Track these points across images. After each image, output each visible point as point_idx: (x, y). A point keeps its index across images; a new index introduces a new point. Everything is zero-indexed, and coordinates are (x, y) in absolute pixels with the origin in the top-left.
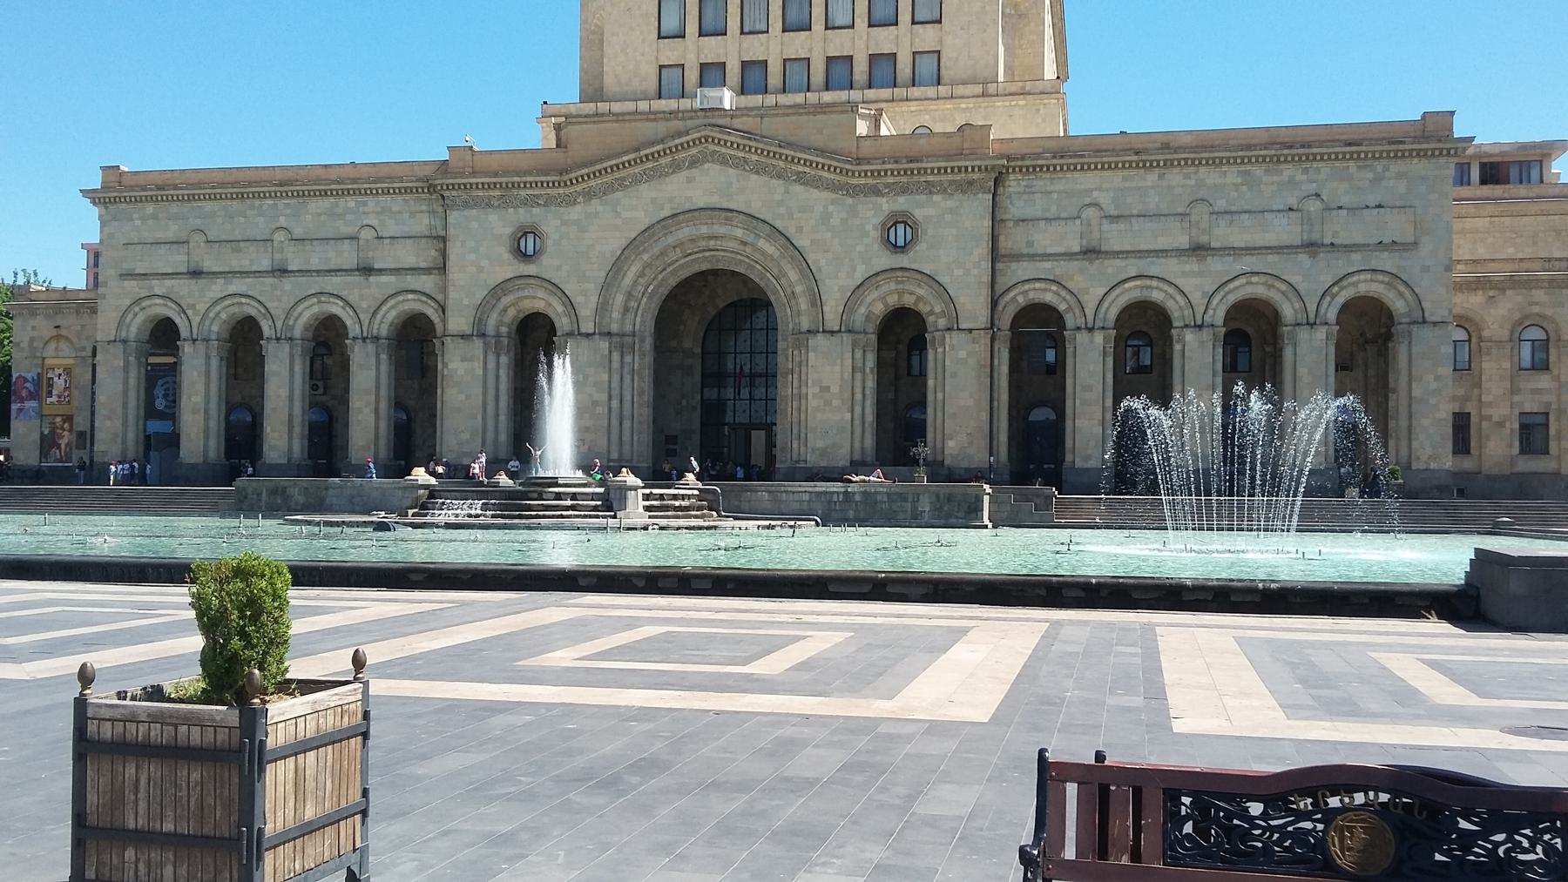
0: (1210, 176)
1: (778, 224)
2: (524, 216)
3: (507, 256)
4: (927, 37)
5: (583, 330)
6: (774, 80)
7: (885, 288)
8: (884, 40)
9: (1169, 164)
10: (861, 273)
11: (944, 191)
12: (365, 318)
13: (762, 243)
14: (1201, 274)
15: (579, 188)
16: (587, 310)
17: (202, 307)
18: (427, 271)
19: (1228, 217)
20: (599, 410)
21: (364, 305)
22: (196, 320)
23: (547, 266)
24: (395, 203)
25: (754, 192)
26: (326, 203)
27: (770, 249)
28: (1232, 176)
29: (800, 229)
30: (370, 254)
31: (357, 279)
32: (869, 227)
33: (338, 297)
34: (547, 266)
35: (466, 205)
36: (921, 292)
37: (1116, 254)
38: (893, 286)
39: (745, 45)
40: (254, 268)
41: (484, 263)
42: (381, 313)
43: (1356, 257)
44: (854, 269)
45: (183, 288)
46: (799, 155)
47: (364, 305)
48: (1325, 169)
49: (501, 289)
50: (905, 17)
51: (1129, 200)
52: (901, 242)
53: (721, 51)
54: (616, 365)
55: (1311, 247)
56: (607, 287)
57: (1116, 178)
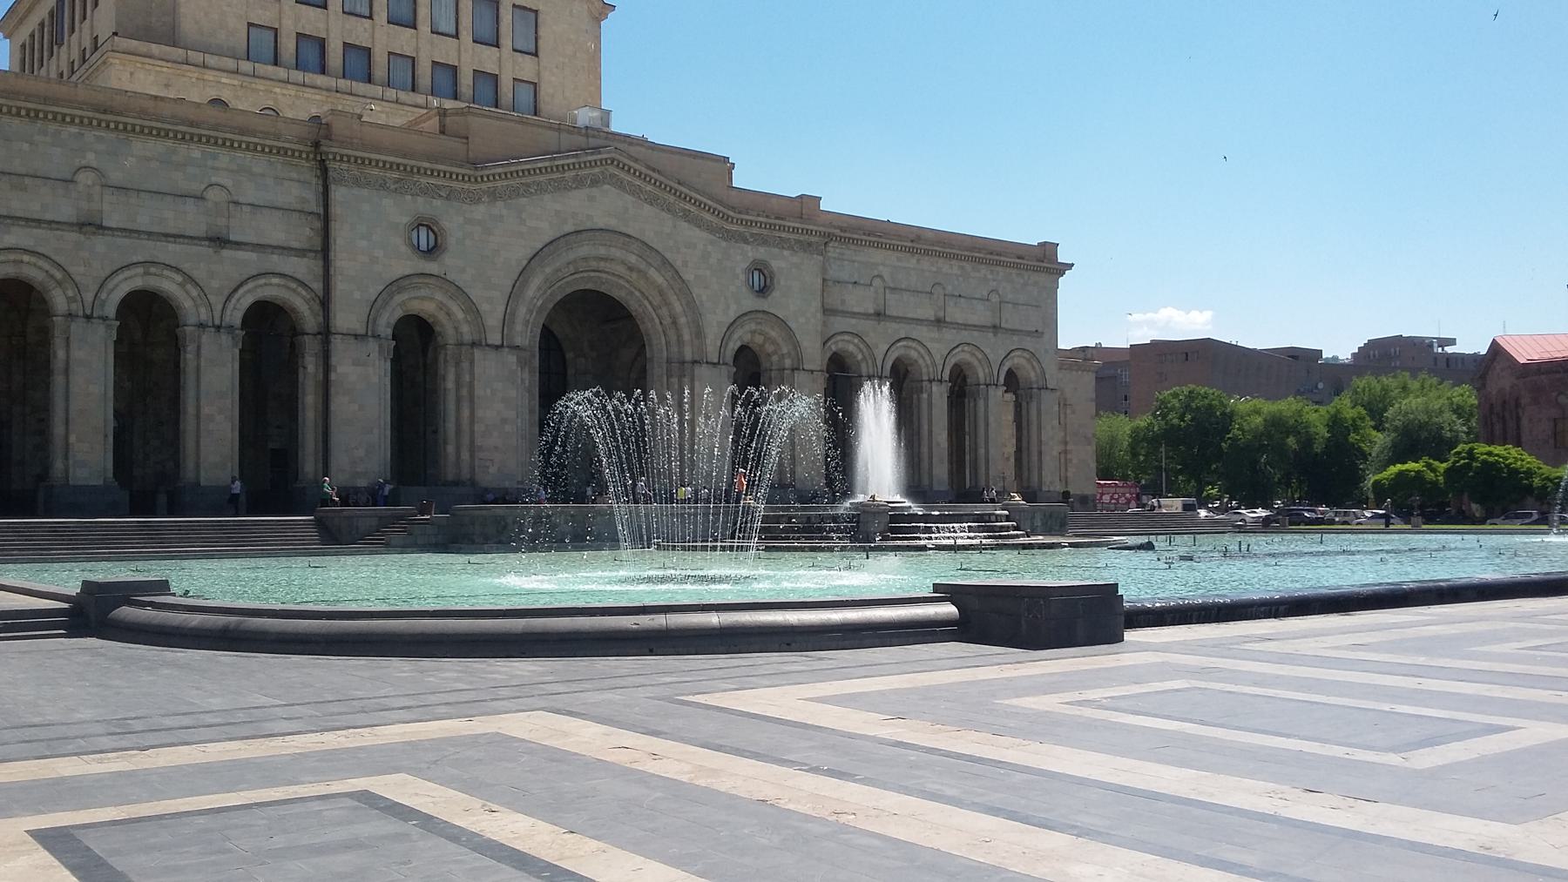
1: (668, 255)
2: (422, 206)
3: (404, 249)
6: (380, 72)
7: (747, 328)
8: (487, 59)
9: (927, 253)
11: (791, 248)
12: (217, 301)
13: (652, 272)
15: (484, 186)
16: (493, 320)
18: (301, 253)
20: (508, 428)
21: (215, 284)
23: (450, 264)
24: (259, 164)
25: (648, 222)
27: (660, 280)
28: (950, 268)
29: (685, 264)
30: (222, 222)
31: (205, 250)
32: (738, 271)
33: (178, 270)
34: (450, 264)
35: (357, 183)
36: (773, 334)
38: (753, 326)
40: (48, 217)
42: (237, 296)
43: (1015, 338)
46: (694, 195)
49: (396, 285)
53: (322, 26)
55: (996, 328)
56: (513, 296)
57: (892, 257)
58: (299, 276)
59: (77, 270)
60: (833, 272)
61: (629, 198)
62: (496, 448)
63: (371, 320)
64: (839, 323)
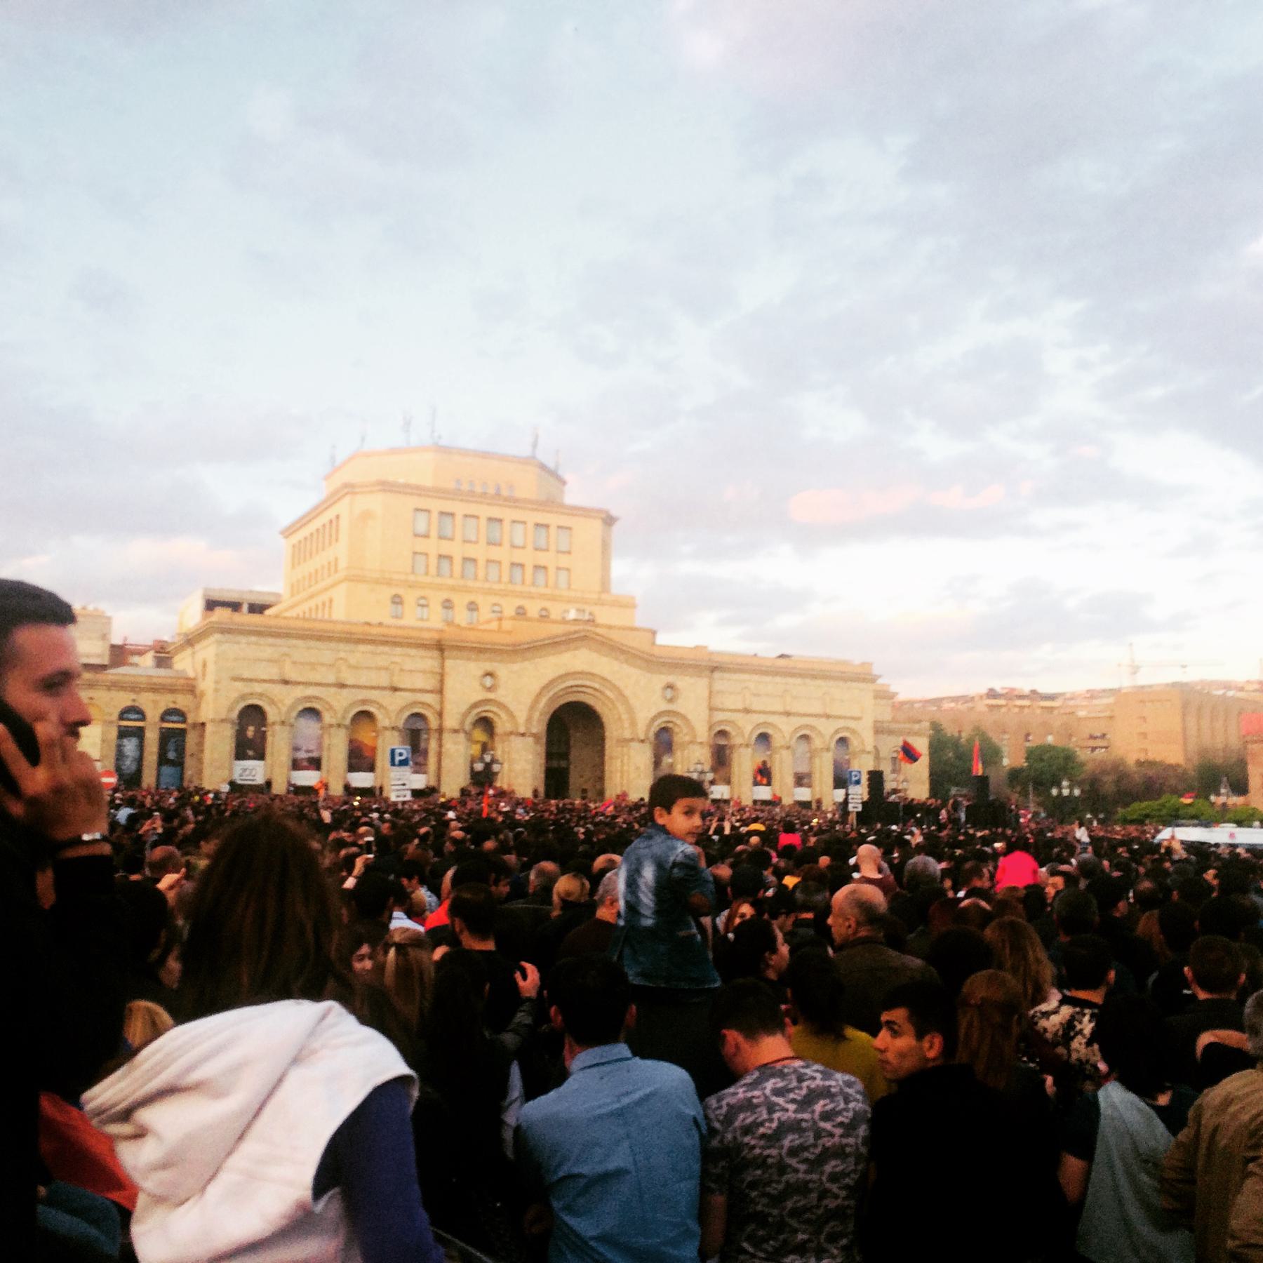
0: (791, 680)
2: (488, 666)
4: (564, 561)
10: (654, 712)
12: (393, 716)
13: (608, 693)
18: (431, 692)
22: (284, 709)
24: (413, 652)
26: (369, 648)
28: (799, 681)
31: (388, 693)
34: (501, 695)
37: (755, 712)
45: (277, 691)
48: (832, 683)
55: (828, 716)
56: (532, 708)
57: (756, 677)
59: (335, 704)
60: (718, 686)
63: (462, 723)
64: (720, 716)
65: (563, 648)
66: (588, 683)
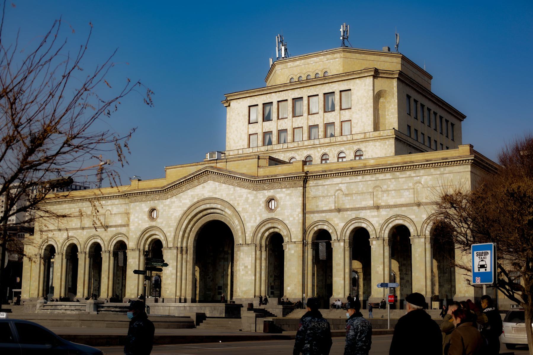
0: (381, 176)
1: (231, 203)
3: (147, 219)
4: (346, 115)
5: (169, 246)
10: (258, 221)
12: (106, 243)
13: (227, 210)
14: (378, 216)
16: (170, 239)
17: (61, 241)
18: (124, 226)
19: (387, 192)
21: (106, 239)
22: (60, 246)
24: (116, 201)
28: (388, 176)
29: (238, 204)
32: (261, 202)
34: (160, 222)
37: (347, 210)
39: (279, 124)
40: (76, 227)
41: (140, 222)
44: (256, 219)
47: (107, 239)
50: (337, 108)
51: (352, 187)
52: (273, 208)
54: (179, 259)
57: (347, 179)
58: (124, 233)
61: (217, 183)
62: (169, 284)
63: (138, 244)
64: (316, 217)
65: (196, 182)
66: (208, 206)
